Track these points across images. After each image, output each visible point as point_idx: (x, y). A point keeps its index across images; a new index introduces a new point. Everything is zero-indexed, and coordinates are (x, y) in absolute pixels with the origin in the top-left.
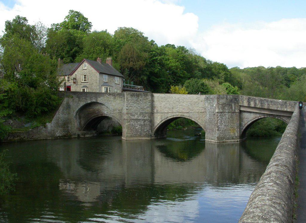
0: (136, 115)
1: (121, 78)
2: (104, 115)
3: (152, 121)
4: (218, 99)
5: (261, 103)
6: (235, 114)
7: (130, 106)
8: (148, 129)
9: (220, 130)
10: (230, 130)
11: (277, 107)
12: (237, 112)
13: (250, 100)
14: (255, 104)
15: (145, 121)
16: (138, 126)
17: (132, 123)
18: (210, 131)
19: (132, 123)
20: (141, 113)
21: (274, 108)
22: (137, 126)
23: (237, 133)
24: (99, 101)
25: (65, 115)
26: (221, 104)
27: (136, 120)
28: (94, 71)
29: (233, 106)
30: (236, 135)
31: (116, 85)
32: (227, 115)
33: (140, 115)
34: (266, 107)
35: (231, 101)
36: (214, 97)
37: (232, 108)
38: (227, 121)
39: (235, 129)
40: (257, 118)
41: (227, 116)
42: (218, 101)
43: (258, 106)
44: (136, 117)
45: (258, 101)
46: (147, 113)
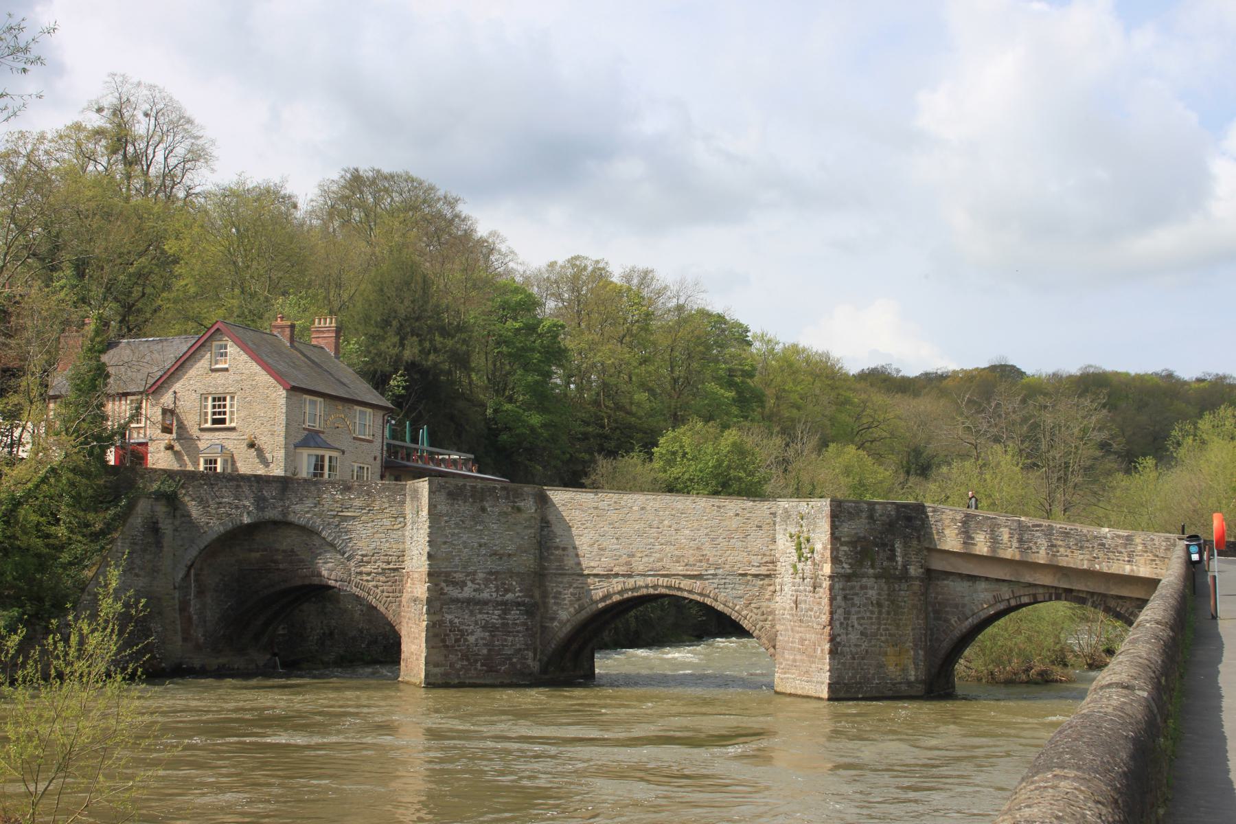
0: (469, 584)
1: (380, 414)
2: (316, 581)
3: (535, 609)
4: (838, 514)
5: (1020, 541)
6: (904, 586)
7: (445, 543)
8: (518, 646)
9: (842, 653)
10: (886, 654)
11: (1088, 560)
12: (917, 578)
13: (972, 524)
14: (995, 541)
15: (505, 612)
16: (479, 633)
18: (798, 657)
19: (449, 617)
20: (491, 573)
21: (1079, 560)
22: (472, 633)
23: (917, 669)
24: (292, 518)
25: (137, 575)
26: (847, 539)
27: (469, 602)
28: (264, 378)
29: (899, 551)
30: (912, 678)
31: (358, 443)
32: (872, 588)
33: (487, 581)
34: (1041, 557)
35: (890, 526)
36: (820, 510)
37: (892, 558)
39: (907, 651)
40: (1002, 606)
41: (870, 592)
42: (834, 527)
43: (1008, 554)
44: (468, 592)
45: (1007, 530)
46: (518, 574)
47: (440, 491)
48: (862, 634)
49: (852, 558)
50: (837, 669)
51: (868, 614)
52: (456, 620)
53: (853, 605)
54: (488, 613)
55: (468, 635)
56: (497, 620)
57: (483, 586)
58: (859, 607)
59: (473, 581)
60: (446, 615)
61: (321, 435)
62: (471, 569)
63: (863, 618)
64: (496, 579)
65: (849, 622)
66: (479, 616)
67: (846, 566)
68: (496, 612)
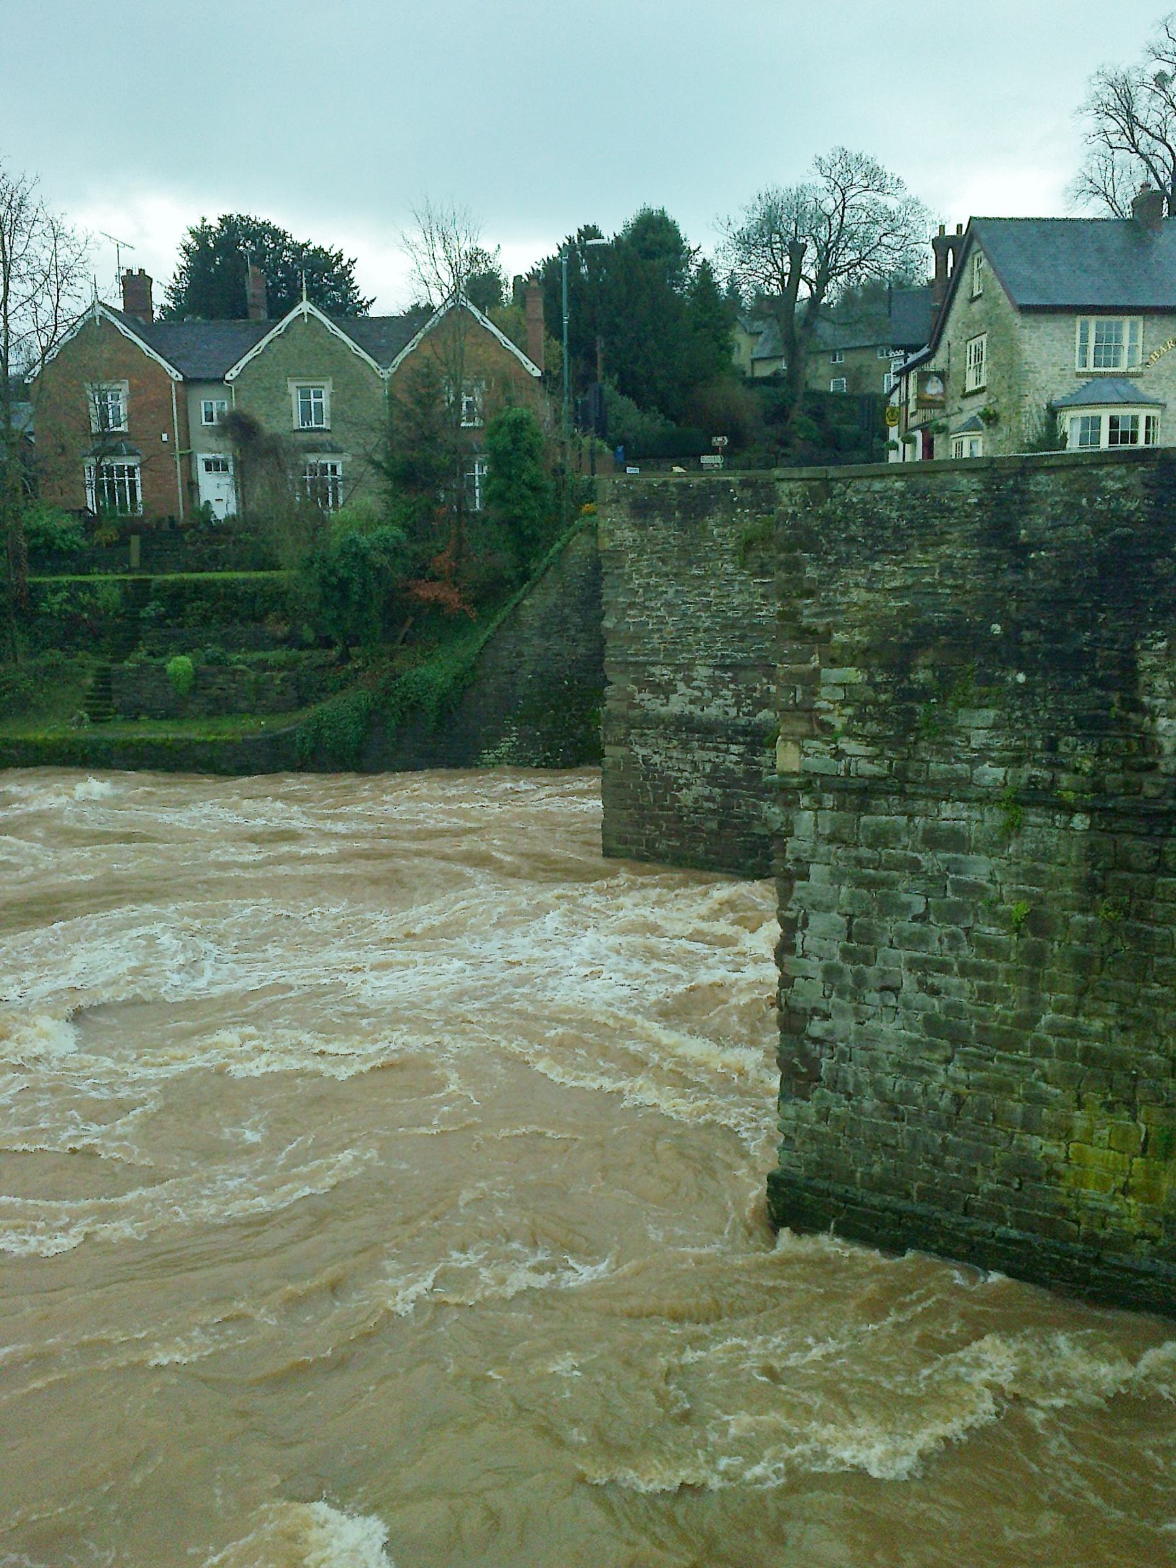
0: (681, 687)
7: (632, 605)
17: (642, 752)
19: (642, 752)
22: (688, 786)
26: (860, 637)
33: (715, 685)
38: (988, 947)
44: (677, 705)
47: (617, 501)
48: (931, 1024)
49: (883, 718)
50: (813, 1136)
51: (968, 953)
52: (656, 759)
53: (890, 907)
54: (716, 749)
55: (680, 789)
56: (737, 763)
57: (708, 694)
58: (922, 918)
59: (688, 681)
60: (637, 748)
61: (1132, 381)
62: (683, 658)
63: (944, 968)
64: (733, 680)
65: (870, 972)
66: (699, 755)
67: (850, 746)
68: (733, 748)
